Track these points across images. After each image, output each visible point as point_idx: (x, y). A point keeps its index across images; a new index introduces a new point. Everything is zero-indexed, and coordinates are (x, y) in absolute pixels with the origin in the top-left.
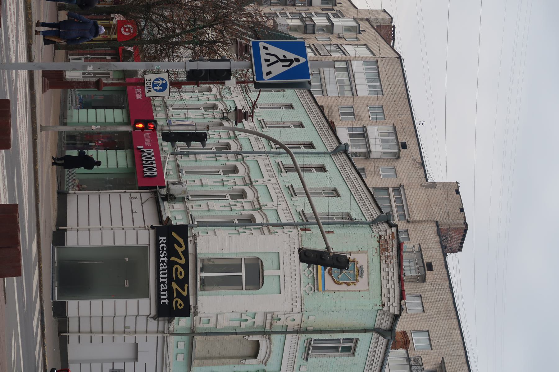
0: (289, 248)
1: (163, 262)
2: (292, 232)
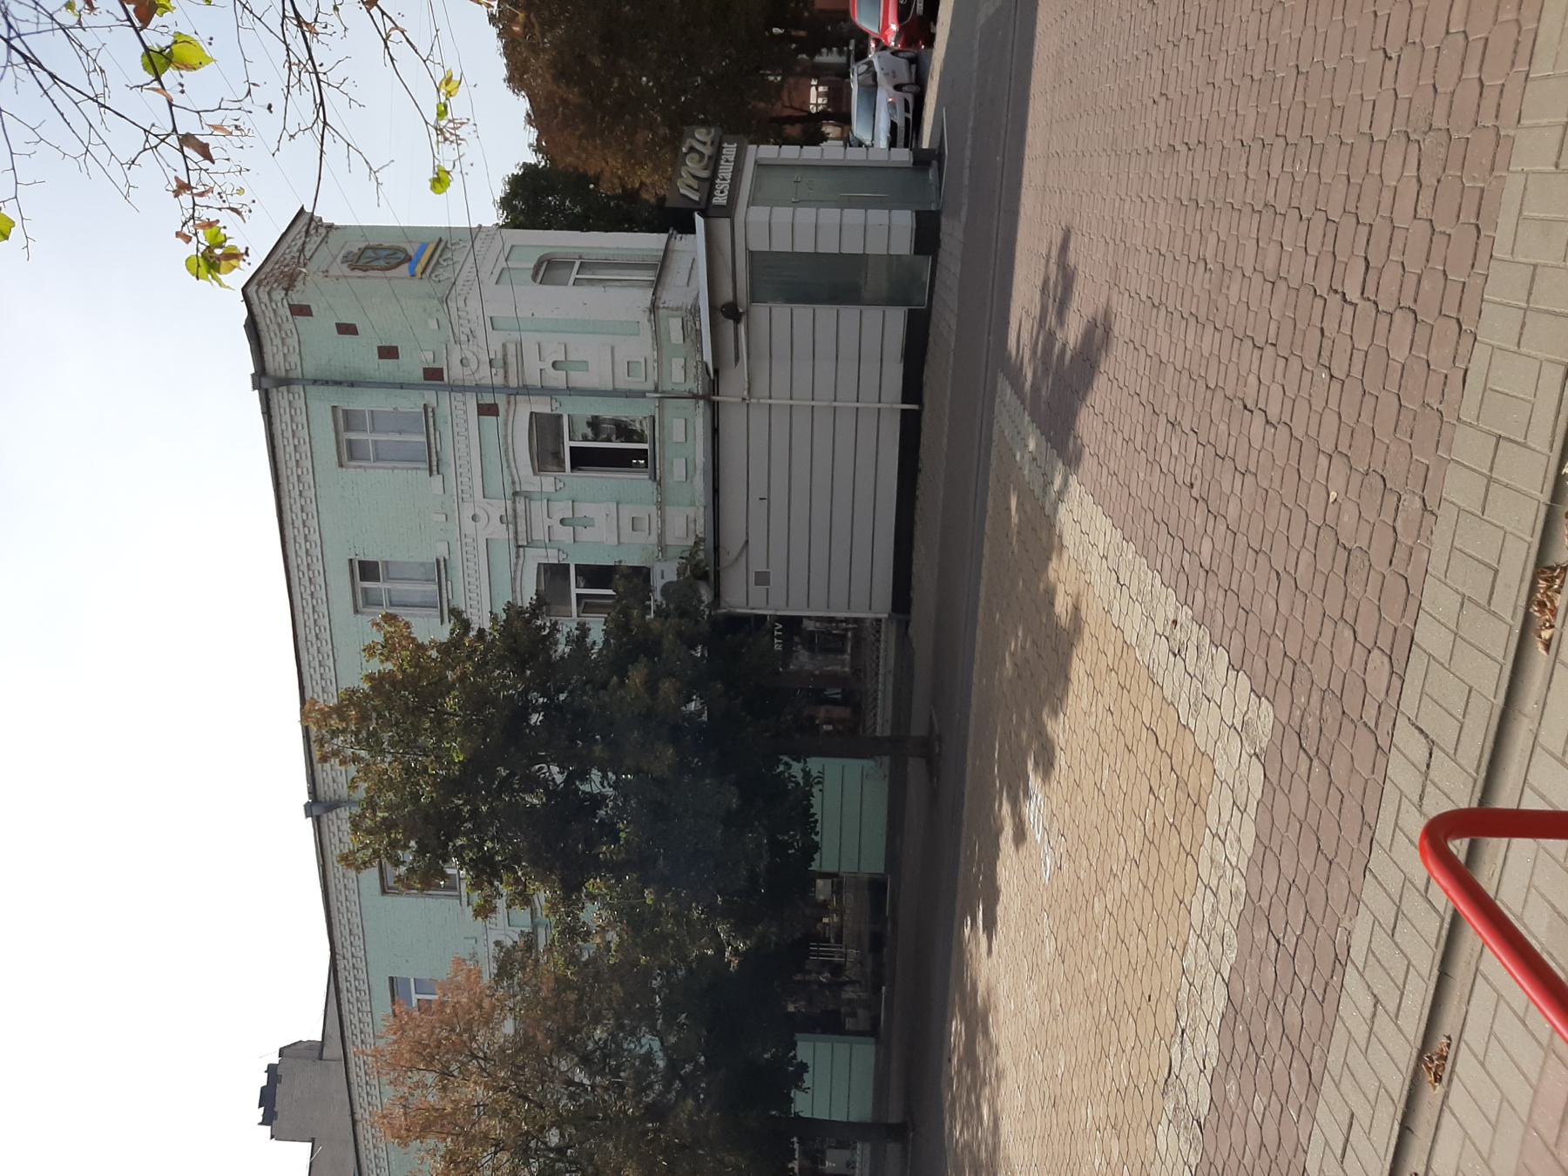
1: (724, 179)
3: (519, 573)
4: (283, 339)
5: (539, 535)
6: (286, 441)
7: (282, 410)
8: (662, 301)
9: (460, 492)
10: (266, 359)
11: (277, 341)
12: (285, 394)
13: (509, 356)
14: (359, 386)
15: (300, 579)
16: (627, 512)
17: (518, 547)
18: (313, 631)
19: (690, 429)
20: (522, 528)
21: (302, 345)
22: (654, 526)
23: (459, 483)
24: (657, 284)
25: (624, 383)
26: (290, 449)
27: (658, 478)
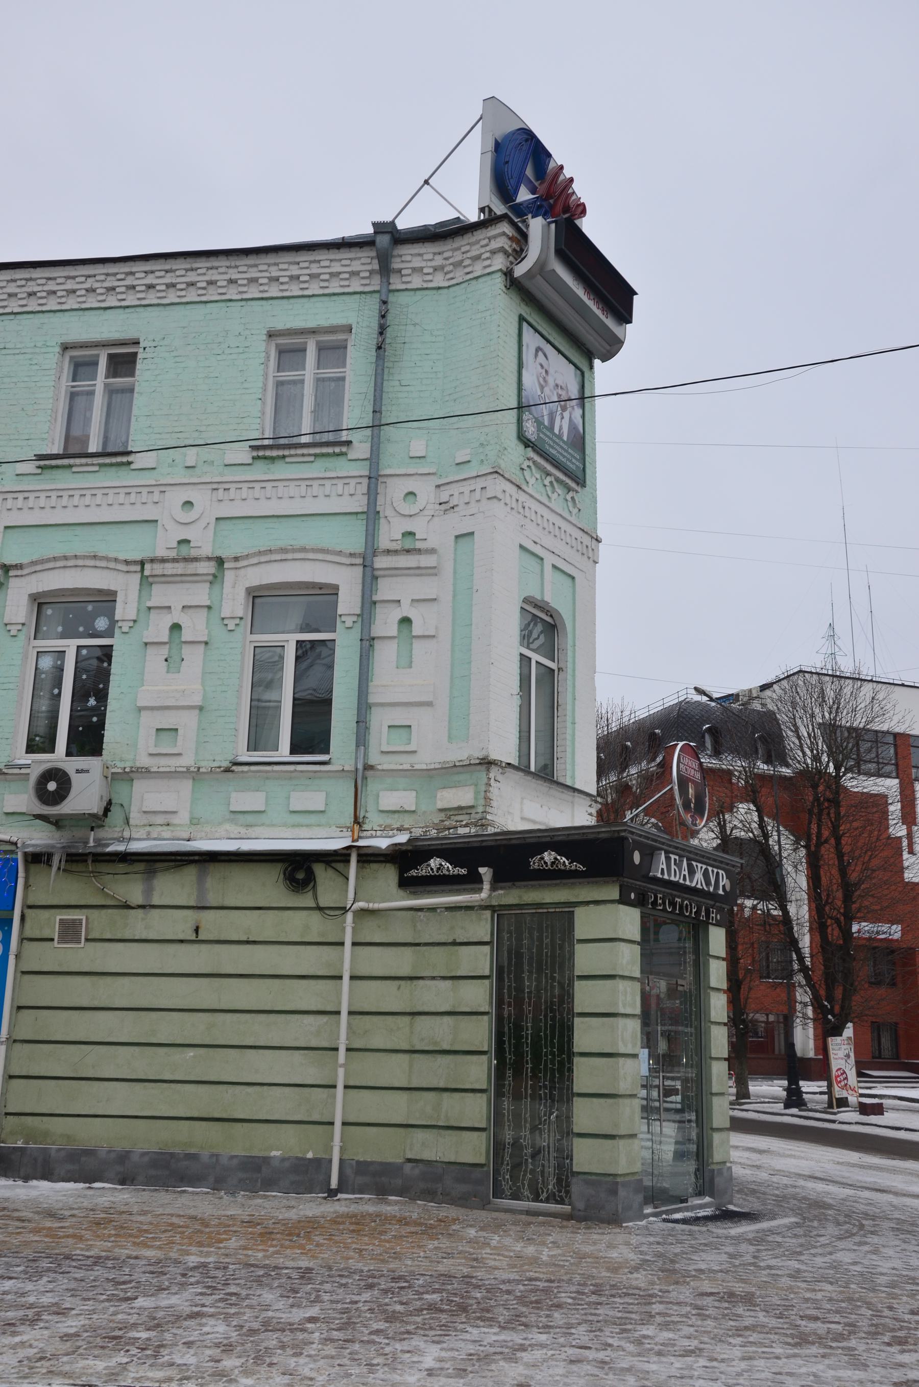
0: (514, 512)
2: (412, 493)
3: (103, 564)
4: (442, 268)
5: (159, 595)
6: (306, 264)
7: (348, 262)
8: (499, 777)
9: (227, 486)
10: (415, 245)
11: (439, 261)
12: (369, 267)
13: (417, 557)
14: (378, 357)
15: (115, 274)
16: (187, 723)
17: (142, 563)
18: (40, 288)
19: (313, 819)
20: (169, 568)
21: (435, 292)
22: (163, 761)
23: (239, 485)
24: (522, 768)
25: (379, 720)
26: (294, 270)
27: (234, 768)
